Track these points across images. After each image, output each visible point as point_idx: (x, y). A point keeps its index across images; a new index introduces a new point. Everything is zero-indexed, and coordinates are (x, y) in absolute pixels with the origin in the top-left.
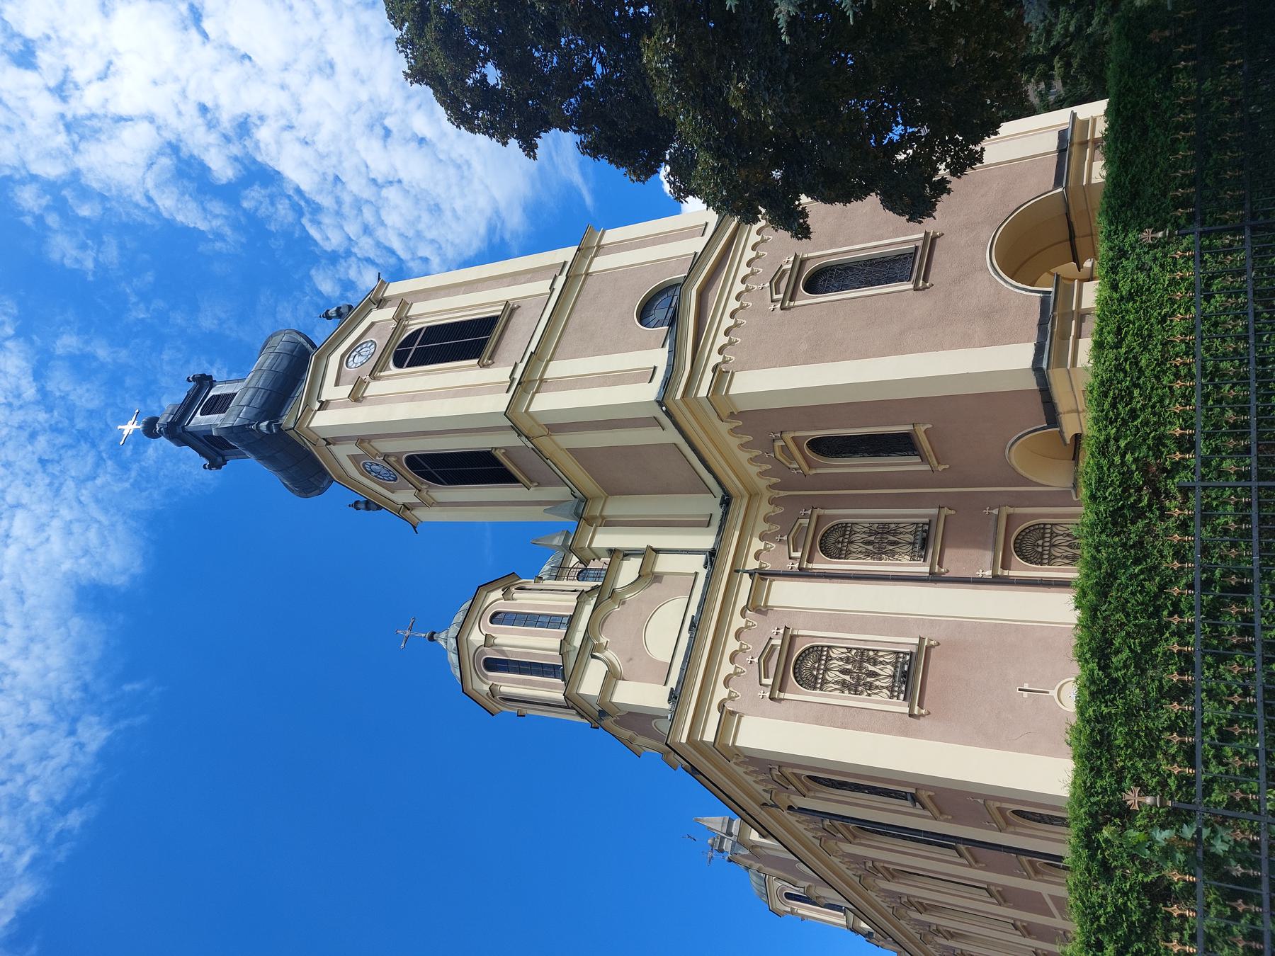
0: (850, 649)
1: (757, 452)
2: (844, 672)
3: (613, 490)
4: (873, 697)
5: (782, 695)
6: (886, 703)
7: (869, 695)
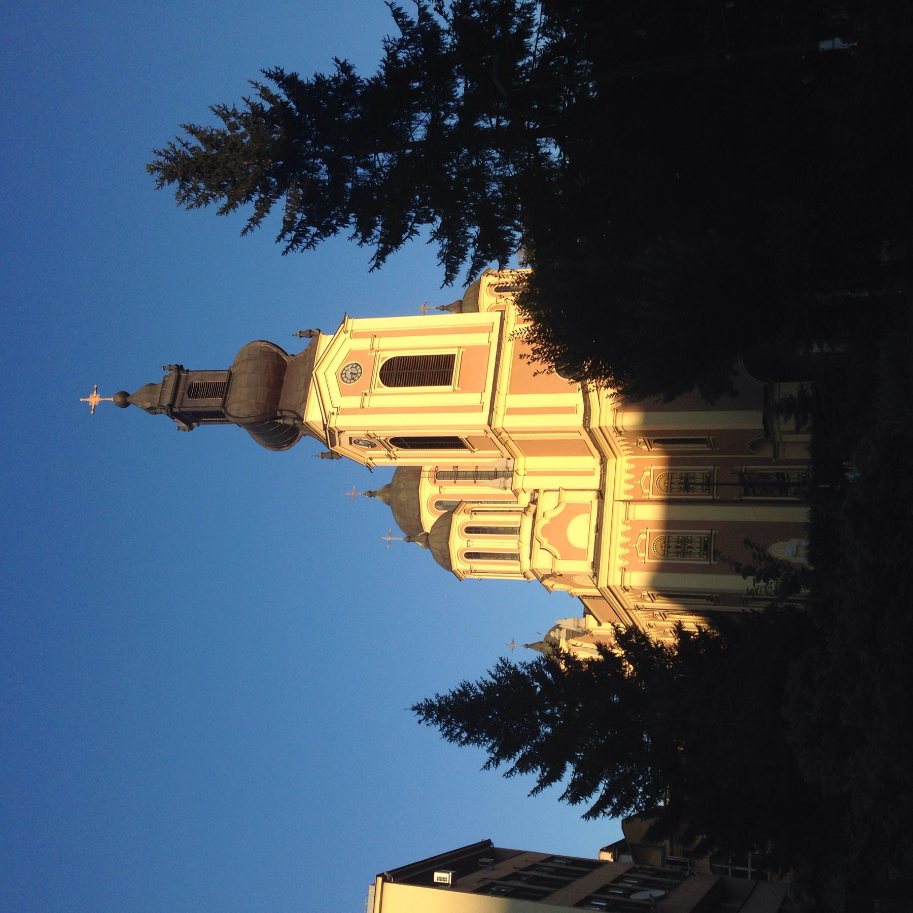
4: (692, 558)
6: (698, 560)
7: (691, 557)
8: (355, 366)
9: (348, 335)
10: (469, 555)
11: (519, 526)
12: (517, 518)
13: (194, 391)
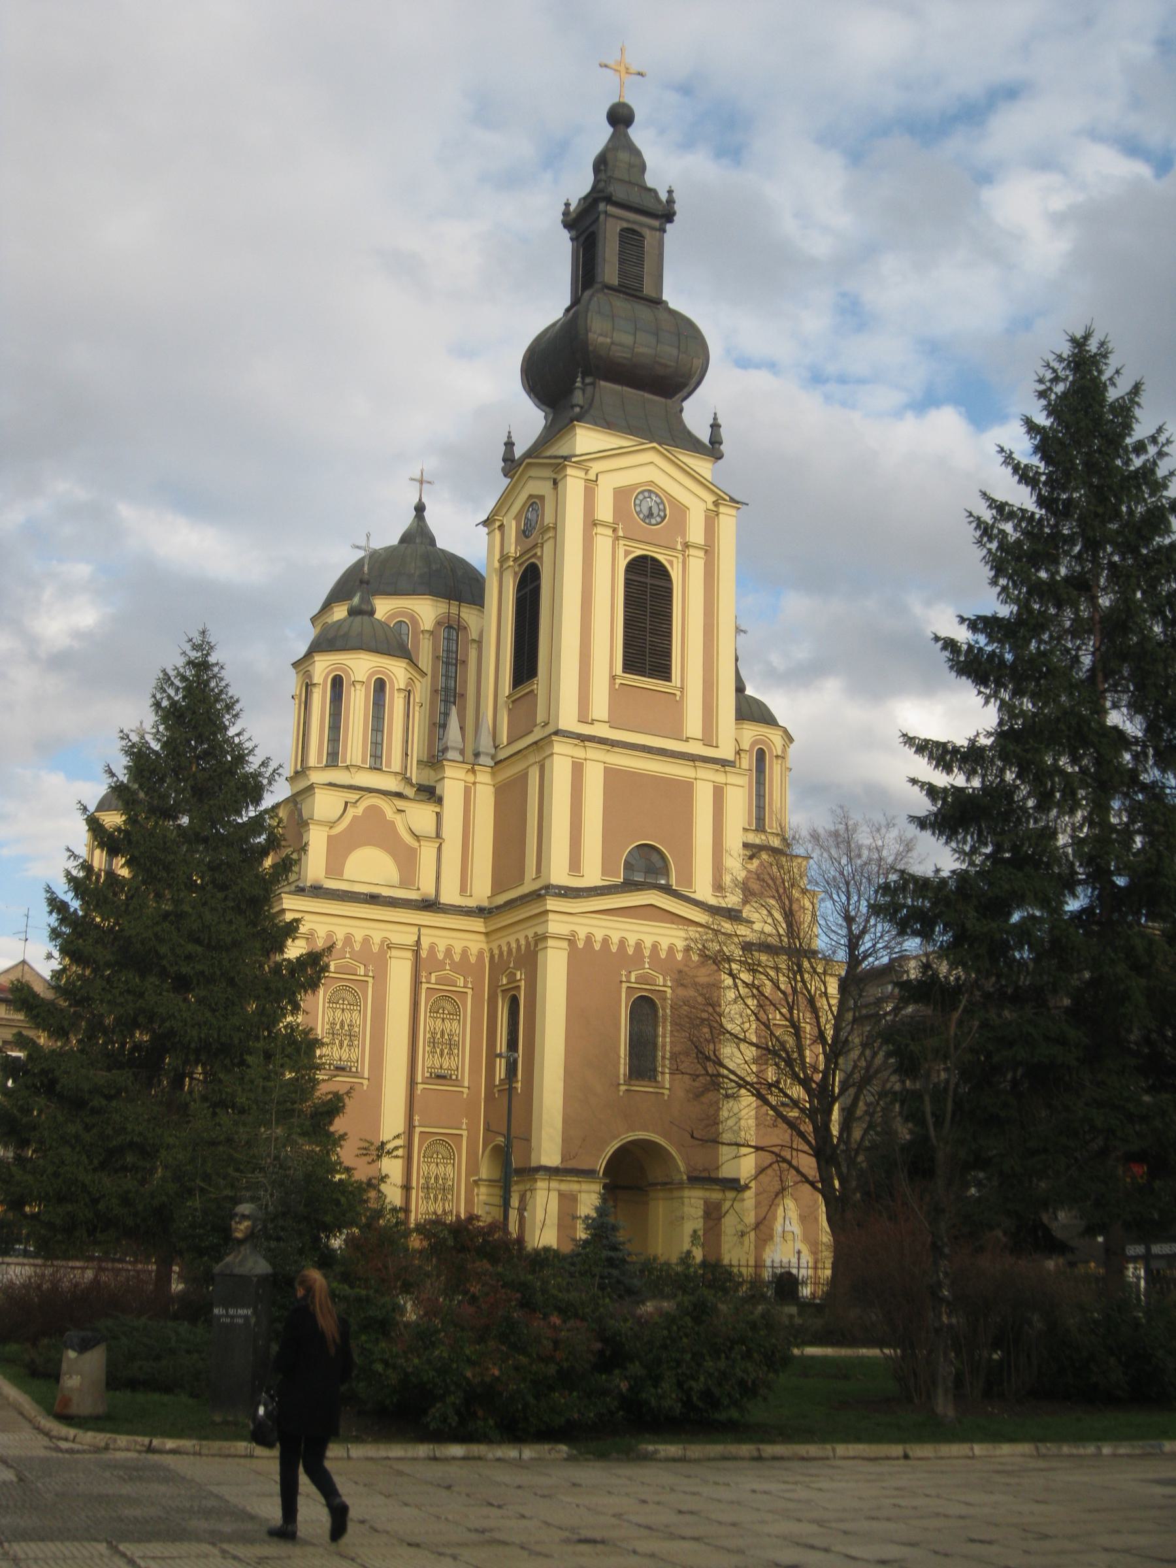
8: (662, 514)
9: (712, 507)
10: (337, 683)
11: (384, 769)
12: (396, 766)
13: (631, 240)
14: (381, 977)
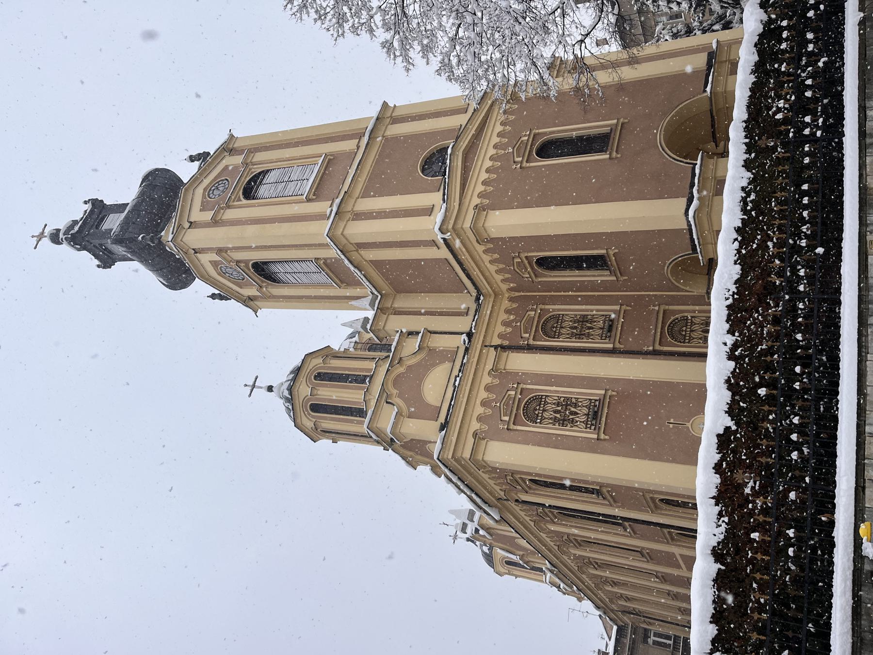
0: (560, 398)
1: (501, 266)
2: (556, 412)
3: (401, 289)
5: (515, 427)
6: (582, 432)
7: (572, 427)
10: (316, 408)
14: (518, 378)
